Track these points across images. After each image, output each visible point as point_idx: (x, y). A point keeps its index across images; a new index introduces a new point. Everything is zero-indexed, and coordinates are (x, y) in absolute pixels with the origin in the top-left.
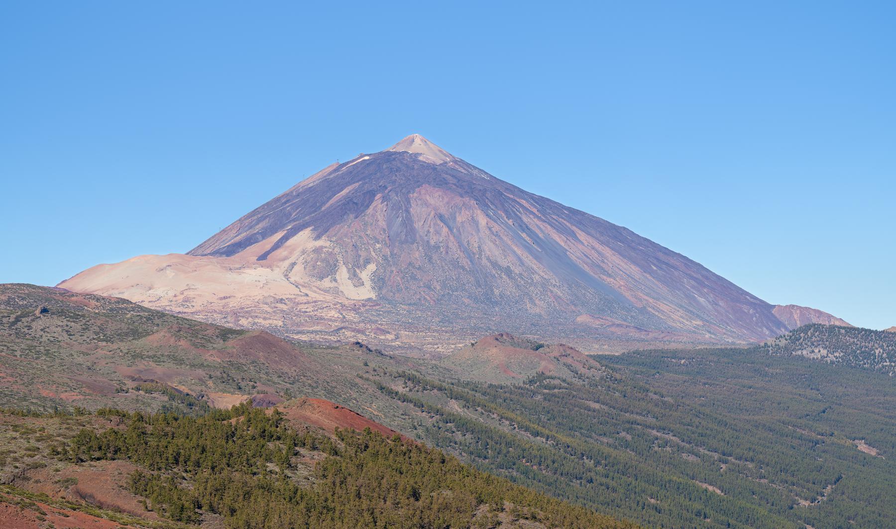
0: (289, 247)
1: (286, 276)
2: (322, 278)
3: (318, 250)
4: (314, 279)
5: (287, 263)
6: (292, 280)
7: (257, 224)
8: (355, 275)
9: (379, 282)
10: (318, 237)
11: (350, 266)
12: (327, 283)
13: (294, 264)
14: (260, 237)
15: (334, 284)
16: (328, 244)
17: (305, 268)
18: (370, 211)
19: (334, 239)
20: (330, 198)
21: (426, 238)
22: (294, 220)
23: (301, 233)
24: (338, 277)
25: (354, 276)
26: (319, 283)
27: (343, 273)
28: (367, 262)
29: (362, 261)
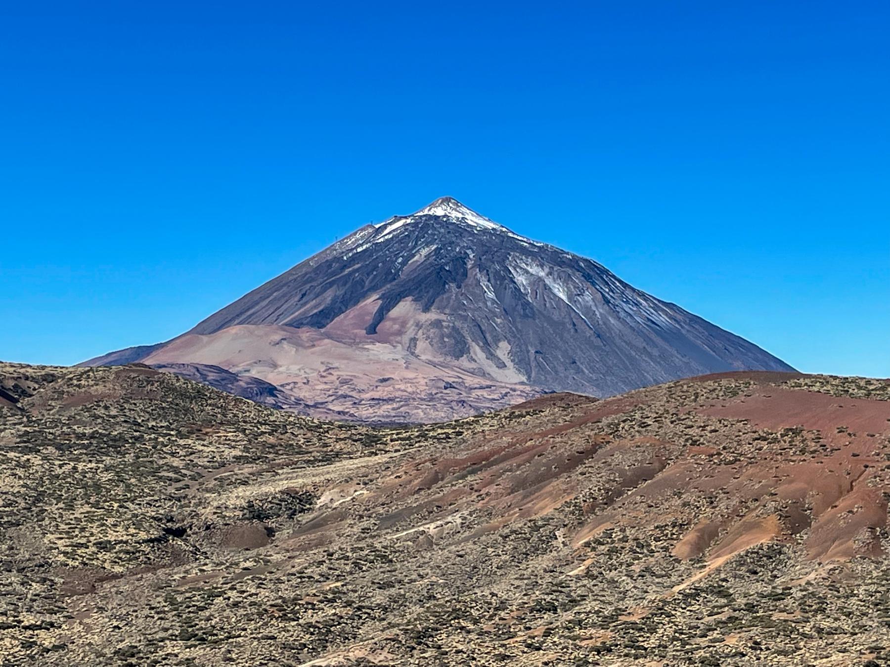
0: (394, 320)
1: (413, 354)
2: (457, 358)
3: (437, 324)
4: (449, 358)
5: (406, 339)
6: (423, 357)
7: (324, 290)
8: (492, 355)
9: (522, 363)
10: (426, 309)
11: (481, 344)
12: (464, 362)
13: (414, 340)
14: (343, 308)
15: (473, 365)
16: (442, 317)
17: (432, 345)
18: (470, 280)
19: (447, 311)
20: (404, 263)
21: (545, 313)
22: (374, 289)
23: (401, 304)
24: (474, 357)
25: (491, 356)
26: (456, 363)
27: (477, 351)
28: (497, 340)
29: (489, 338)
